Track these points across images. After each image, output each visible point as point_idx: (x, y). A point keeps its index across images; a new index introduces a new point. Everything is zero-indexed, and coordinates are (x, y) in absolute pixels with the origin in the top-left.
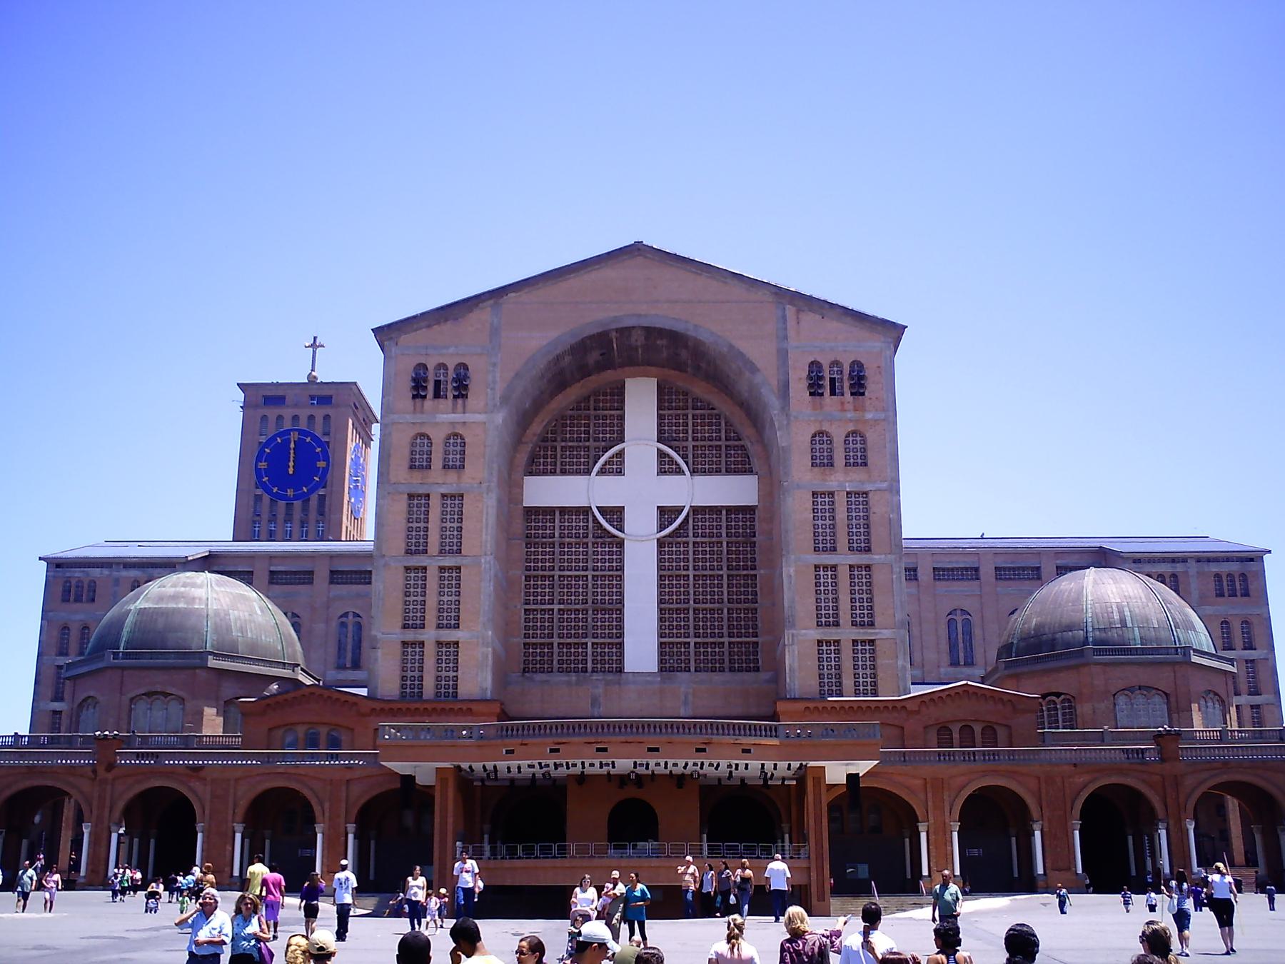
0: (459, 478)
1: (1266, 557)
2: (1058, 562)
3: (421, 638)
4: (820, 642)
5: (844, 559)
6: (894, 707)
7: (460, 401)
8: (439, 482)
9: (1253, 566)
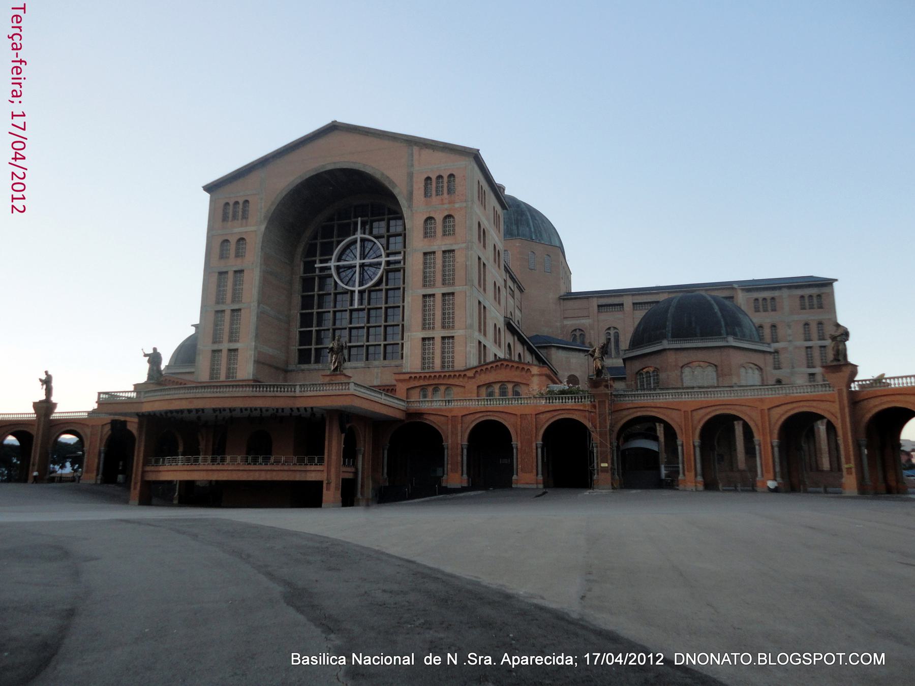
1: (835, 284)
3: (220, 348)
4: (424, 339)
5: (439, 291)
7: (244, 221)
9: (825, 290)
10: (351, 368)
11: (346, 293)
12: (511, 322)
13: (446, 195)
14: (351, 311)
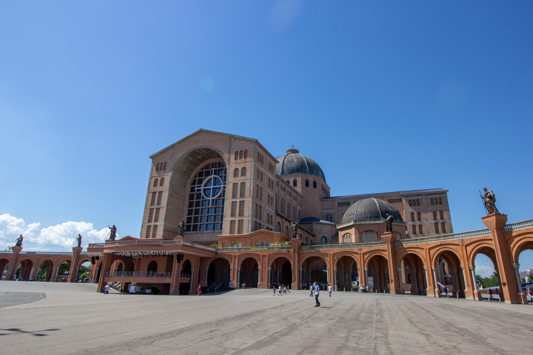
0: (162, 188)
2: (389, 198)
6: (244, 237)
7: (164, 170)
8: (159, 189)
9: (442, 195)
10: (207, 233)
11: (207, 200)
12: (278, 212)
13: (243, 159)
14: (209, 208)
